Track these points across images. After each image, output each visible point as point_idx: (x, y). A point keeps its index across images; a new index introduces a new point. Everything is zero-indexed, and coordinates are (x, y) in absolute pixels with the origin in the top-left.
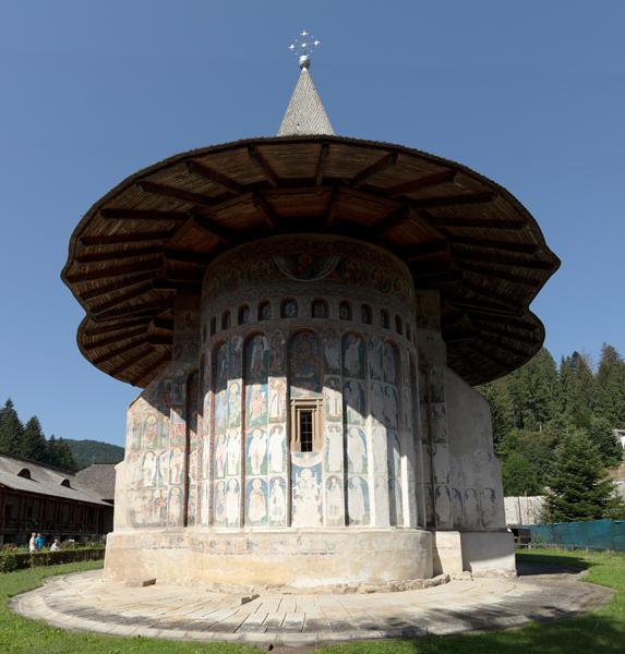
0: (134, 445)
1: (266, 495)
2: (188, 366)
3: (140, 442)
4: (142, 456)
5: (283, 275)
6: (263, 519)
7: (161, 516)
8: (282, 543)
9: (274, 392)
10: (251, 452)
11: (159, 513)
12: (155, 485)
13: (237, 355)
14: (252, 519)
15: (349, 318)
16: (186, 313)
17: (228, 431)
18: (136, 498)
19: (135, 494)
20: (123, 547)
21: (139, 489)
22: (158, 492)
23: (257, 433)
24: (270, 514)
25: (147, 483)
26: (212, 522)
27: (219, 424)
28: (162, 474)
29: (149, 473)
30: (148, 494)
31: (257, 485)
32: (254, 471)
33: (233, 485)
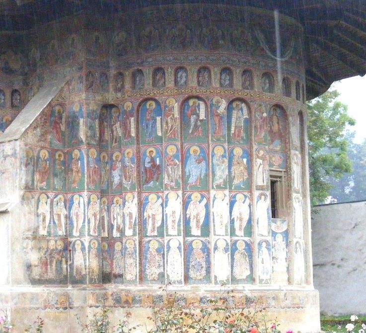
1: (251, 256)
2: (99, 98)
3: (33, 180)
4: (36, 198)
5: (263, 49)
6: (247, 277)
8: (274, 298)
9: (259, 161)
10: (235, 214)
11: (54, 264)
12: (49, 233)
13: (221, 118)
14: (238, 277)
16: (96, 33)
17: (213, 192)
19: (31, 244)
20: (27, 306)
21: (35, 238)
23: (240, 197)
24: (259, 273)
25: (43, 232)
26: (187, 278)
27: (192, 180)
28: (56, 222)
29: (44, 220)
30: (44, 245)
31: (241, 246)
32: (238, 232)
33: (222, 244)
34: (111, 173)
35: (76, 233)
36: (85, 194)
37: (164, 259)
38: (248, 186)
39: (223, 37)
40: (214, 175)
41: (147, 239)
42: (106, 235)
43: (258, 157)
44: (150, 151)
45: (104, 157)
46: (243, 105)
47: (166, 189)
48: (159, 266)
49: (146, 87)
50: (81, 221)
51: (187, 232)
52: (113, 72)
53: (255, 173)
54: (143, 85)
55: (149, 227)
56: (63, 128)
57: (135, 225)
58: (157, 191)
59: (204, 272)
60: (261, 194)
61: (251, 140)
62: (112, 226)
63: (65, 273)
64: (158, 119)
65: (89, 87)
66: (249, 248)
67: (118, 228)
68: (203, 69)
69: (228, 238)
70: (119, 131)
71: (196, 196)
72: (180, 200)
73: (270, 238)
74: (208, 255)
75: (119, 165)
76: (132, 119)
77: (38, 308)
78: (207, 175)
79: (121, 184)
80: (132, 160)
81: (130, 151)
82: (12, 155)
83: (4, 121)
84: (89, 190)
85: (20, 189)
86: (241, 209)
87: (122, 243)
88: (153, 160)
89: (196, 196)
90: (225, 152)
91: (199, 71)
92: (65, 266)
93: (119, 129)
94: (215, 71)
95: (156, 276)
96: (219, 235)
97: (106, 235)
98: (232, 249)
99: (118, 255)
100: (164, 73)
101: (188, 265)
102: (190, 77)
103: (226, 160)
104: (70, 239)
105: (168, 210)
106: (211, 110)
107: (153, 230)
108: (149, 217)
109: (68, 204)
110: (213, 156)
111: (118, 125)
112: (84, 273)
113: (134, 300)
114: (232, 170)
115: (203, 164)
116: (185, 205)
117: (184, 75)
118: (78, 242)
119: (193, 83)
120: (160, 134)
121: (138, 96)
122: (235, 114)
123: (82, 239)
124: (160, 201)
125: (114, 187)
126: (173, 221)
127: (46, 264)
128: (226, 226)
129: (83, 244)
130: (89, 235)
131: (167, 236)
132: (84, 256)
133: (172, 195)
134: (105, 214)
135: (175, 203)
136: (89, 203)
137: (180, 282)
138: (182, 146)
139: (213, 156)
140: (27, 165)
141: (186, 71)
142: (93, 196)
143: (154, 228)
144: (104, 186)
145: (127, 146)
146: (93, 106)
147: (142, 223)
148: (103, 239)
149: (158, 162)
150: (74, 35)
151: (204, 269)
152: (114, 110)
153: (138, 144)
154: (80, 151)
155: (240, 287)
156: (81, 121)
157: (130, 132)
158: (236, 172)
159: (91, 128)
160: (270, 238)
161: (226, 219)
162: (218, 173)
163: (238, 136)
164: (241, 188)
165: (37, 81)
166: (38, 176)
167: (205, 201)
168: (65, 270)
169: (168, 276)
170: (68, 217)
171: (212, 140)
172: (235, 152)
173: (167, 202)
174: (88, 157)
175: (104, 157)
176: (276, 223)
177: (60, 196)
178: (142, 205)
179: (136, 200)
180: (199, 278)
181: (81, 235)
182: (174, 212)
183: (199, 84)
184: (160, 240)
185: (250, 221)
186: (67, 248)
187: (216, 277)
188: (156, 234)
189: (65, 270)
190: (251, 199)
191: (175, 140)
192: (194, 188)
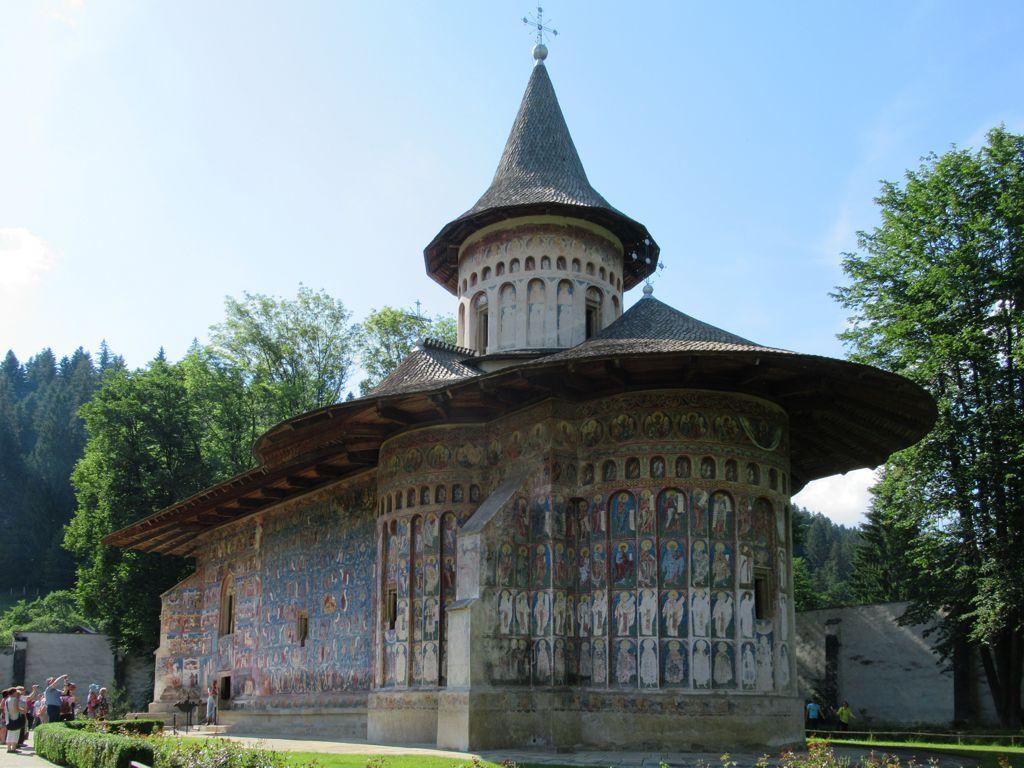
0: (488, 579)
2: (567, 491)
4: (498, 595)
6: (729, 681)
7: (519, 671)
9: (744, 558)
10: (717, 615)
11: (516, 665)
12: (511, 631)
15: (756, 482)
16: (563, 423)
17: (691, 589)
18: (493, 648)
19: (492, 643)
22: (514, 642)
23: (721, 595)
24: (741, 677)
25: (505, 630)
26: (663, 682)
27: (669, 577)
28: (519, 620)
29: (506, 617)
30: (505, 644)
31: (722, 648)
32: (719, 634)
33: (701, 646)
34: (578, 570)
35: (540, 632)
36: (551, 589)
37: (636, 659)
38: (730, 584)
39: (705, 425)
40: (693, 572)
41: (618, 639)
42: (573, 635)
43: (743, 554)
44: (622, 546)
45: (571, 553)
46: (726, 498)
47: (640, 586)
48: (631, 668)
49: (618, 478)
50: (546, 619)
51: (663, 632)
52: (583, 464)
53: (738, 570)
54: (615, 477)
55: (621, 627)
56: (526, 521)
57: (605, 624)
58: (629, 588)
59: (681, 676)
60: (746, 593)
61: (734, 535)
62: (579, 625)
63: (527, 674)
64: (632, 512)
65: (556, 479)
66: (731, 650)
67: (585, 629)
68: (683, 460)
69: (708, 639)
70: (587, 526)
71: (673, 594)
72: (655, 598)
73: (754, 640)
74: (687, 656)
75: (587, 561)
76: (603, 513)
77: (499, 711)
78: (685, 572)
79: (589, 581)
80: (602, 556)
81: (599, 547)
82: (473, 549)
83: (462, 516)
84: (555, 587)
85: (480, 584)
86: (724, 608)
87: (590, 643)
88: (625, 556)
89: (673, 594)
90: (706, 547)
91: (677, 463)
92: (527, 667)
93: (587, 524)
94: (696, 462)
95: (627, 678)
96: (698, 637)
97: (573, 635)
98: (712, 651)
99: (584, 656)
100: (638, 462)
101: (664, 668)
102: (667, 467)
103: (707, 556)
104: (533, 639)
105: (642, 609)
106: (691, 504)
107: (625, 630)
108: (620, 616)
109: (532, 602)
110: (692, 552)
111: (586, 519)
112: (548, 674)
113: (603, 703)
114: (714, 566)
115: (681, 559)
116: (661, 604)
117: (661, 465)
118: (543, 642)
119: (671, 472)
120: (633, 528)
121: (610, 488)
122: (716, 507)
123: (547, 639)
124: (633, 597)
125: (581, 584)
126: (648, 621)
127: (508, 665)
128: (707, 627)
129: (547, 643)
130: (554, 634)
131: (641, 635)
132: (549, 655)
133: (647, 593)
134: (571, 612)
135: (650, 602)
136: (555, 600)
137: (654, 686)
138: (658, 539)
139: (692, 552)
140: (488, 560)
141: (663, 461)
142: (560, 594)
143: (626, 627)
144: (570, 583)
145: (597, 539)
146: (560, 499)
147: (612, 622)
148: (570, 638)
149: (631, 558)
150: (539, 425)
151: (681, 672)
152: (582, 504)
153: (609, 538)
154: (546, 546)
155: (721, 692)
156: (547, 514)
157: (599, 526)
158: (718, 568)
159: (557, 521)
160: (754, 640)
161: (706, 620)
162: (698, 570)
163: (720, 531)
164: (722, 586)
165: (498, 476)
166: (500, 571)
167: (682, 599)
168: (527, 670)
169: (641, 679)
170: (532, 616)
171: (691, 534)
172: (716, 548)
173: (640, 600)
174: (554, 552)
175: (571, 553)
176: (760, 624)
177: (524, 593)
178: (612, 603)
179: (606, 598)
180: (675, 681)
181: (546, 633)
182: (648, 611)
183: (678, 476)
184: (632, 640)
185: (733, 620)
186: (530, 647)
187: (695, 681)
188: (627, 633)
189: (527, 670)
190: (734, 598)
191: (649, 534)
192: (671, 586)
